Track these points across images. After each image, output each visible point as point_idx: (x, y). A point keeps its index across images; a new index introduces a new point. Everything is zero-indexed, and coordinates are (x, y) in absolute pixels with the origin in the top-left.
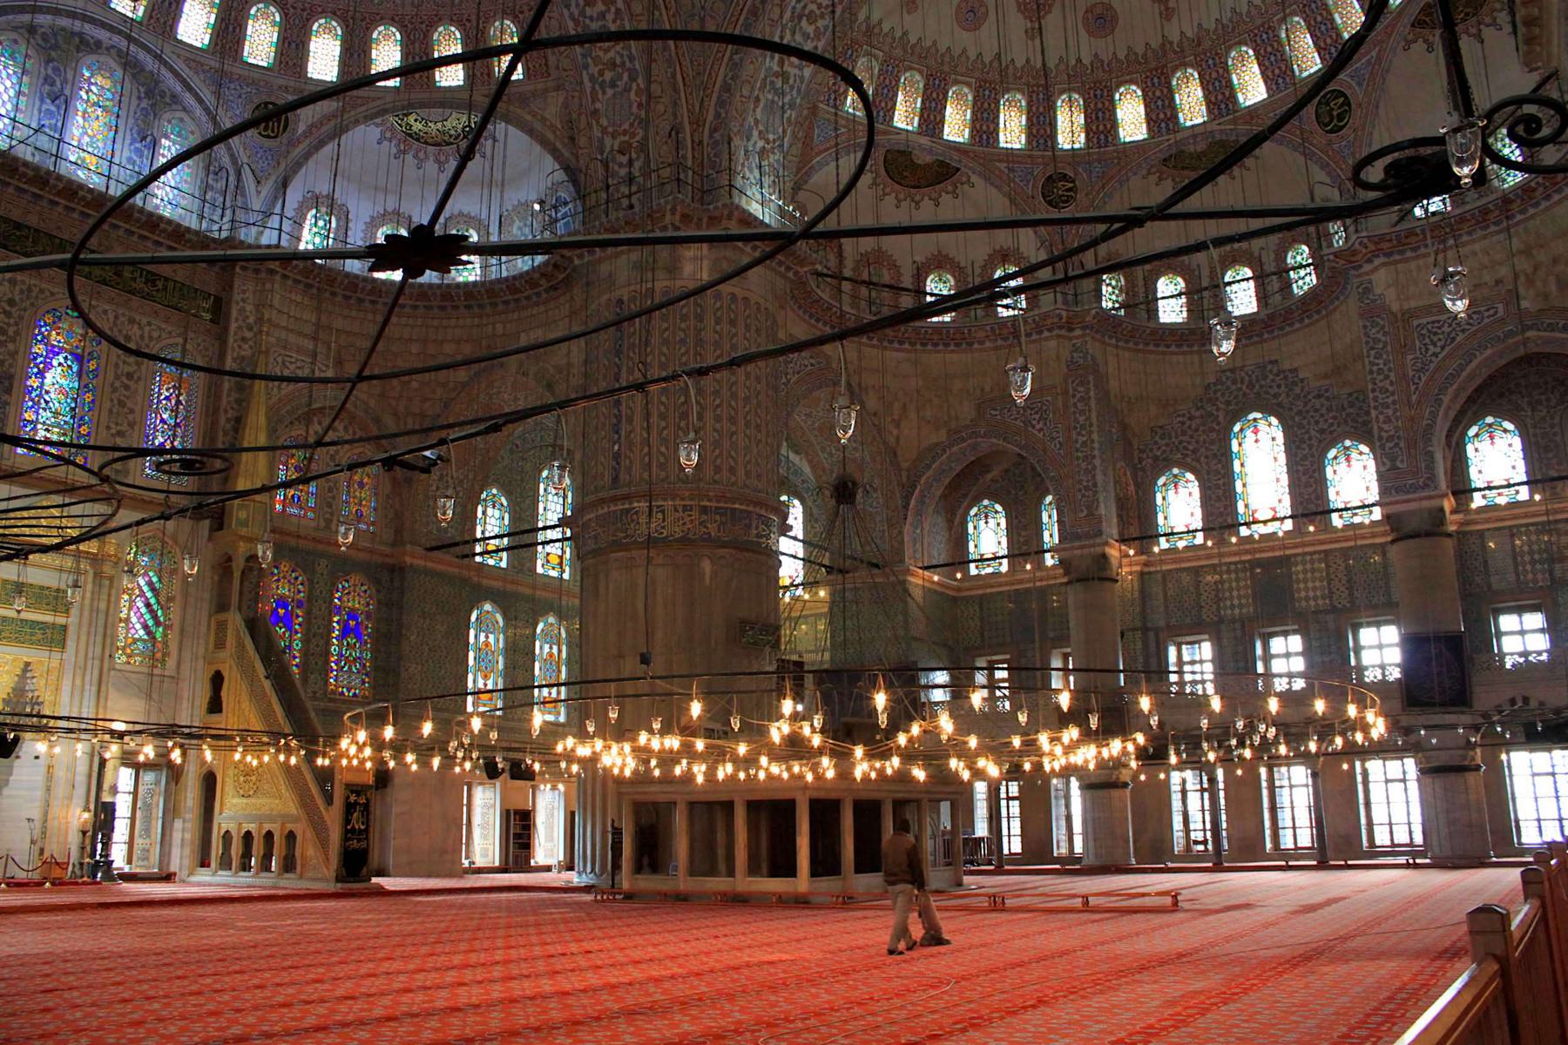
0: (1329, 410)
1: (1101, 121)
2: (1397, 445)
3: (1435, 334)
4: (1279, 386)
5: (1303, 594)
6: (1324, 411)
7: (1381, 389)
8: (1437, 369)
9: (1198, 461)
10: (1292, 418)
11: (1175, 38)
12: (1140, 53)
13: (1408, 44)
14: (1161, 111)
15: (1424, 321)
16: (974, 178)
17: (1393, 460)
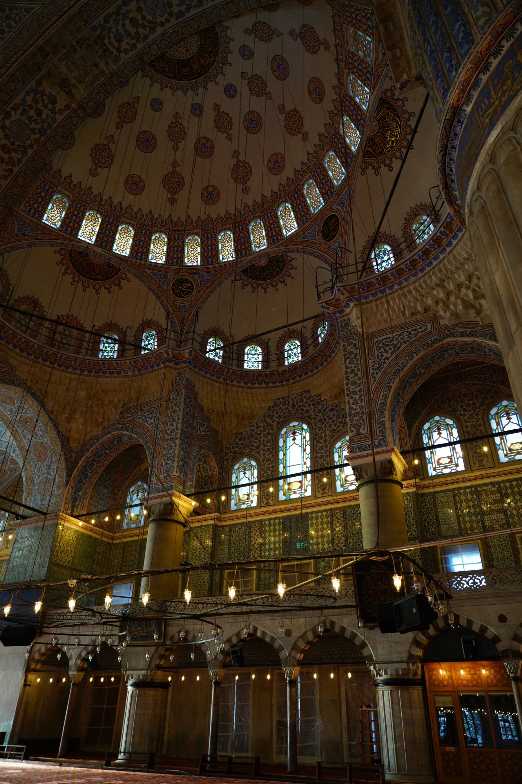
0: (338, 417)
1: (210, 252)
2: (361, 418)
3: (388, 345)
4: (309, 405)
5: (315, 540)
6: (335, 418)
7: (352, 382)
8: (389, 366)
9: (259, 453)
10: (316, 424)
11: (250, 204)
12: (233, 213)
13: (364, 169)
14: (242, 245)
15: (381, 338)
16: (130, 276)
17: (358, 429)
